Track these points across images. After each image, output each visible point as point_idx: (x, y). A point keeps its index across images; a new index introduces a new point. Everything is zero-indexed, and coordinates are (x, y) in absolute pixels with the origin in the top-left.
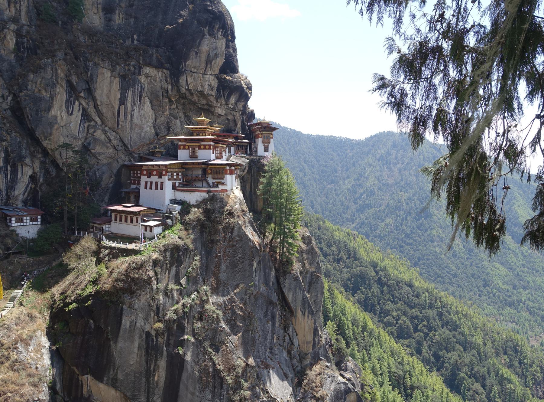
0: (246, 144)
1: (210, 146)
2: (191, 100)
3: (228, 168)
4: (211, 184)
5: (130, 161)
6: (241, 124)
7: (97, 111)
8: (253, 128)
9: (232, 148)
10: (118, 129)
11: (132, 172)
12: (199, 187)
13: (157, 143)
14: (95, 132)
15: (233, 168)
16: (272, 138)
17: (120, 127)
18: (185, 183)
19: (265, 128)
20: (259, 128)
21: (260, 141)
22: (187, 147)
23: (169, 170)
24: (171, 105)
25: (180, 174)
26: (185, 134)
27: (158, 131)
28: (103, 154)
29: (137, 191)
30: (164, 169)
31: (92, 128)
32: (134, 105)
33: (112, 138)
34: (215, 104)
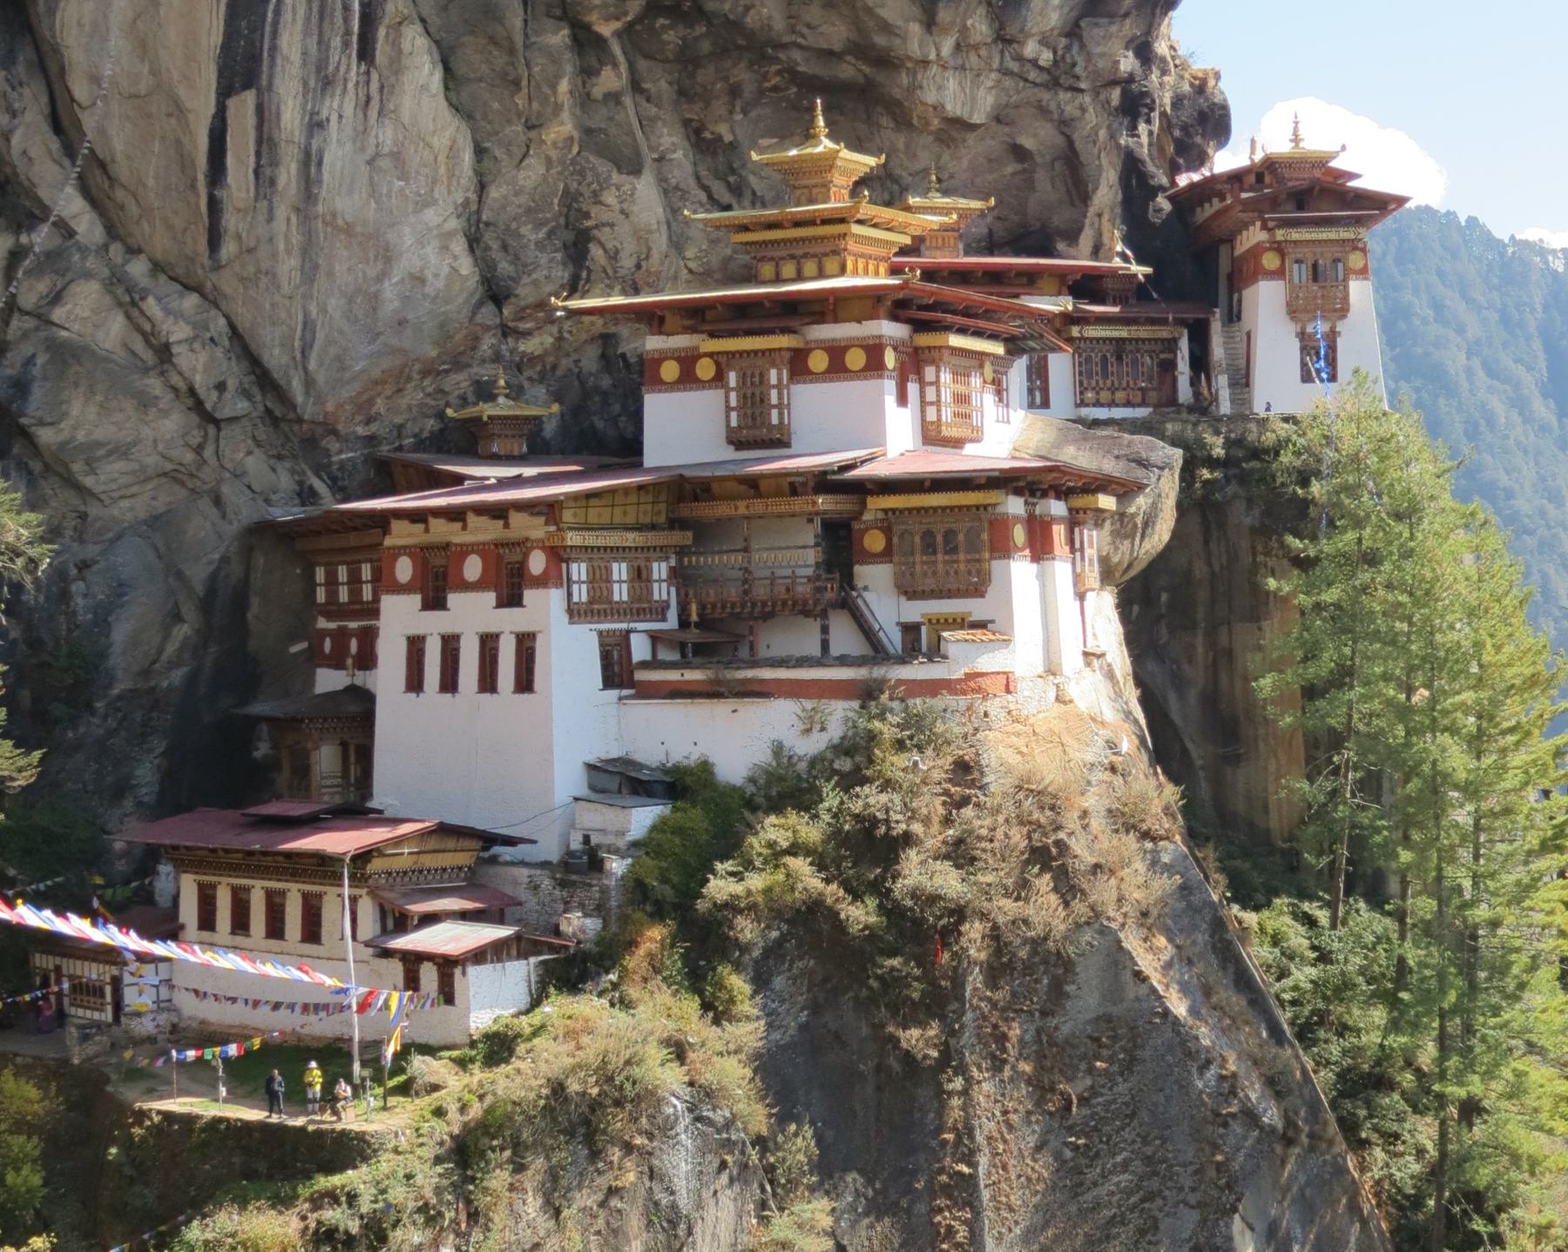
0: (1164, 332)
1: (874, 351)
2: (735, 26)
3: (1015, 506)
4: (893, 639)
5: (306, 495)
7: (70, 151)
8: (1208, 211)
10: (217, 267)
11: (320, 575)
12: (803, 662)
13: (497, 358)
14: (56, 298)
15: (1057, 508)
16: (1363, 272)
17: (228, 249)
18: (693, 636)
19: (1301, 198)
21: (1266, 302)
22: (705, 369)
23: (573, 539)
24: (587, 72)
26: (704, 278)
27: (504, 267)
28: (121, 451)
29: (354, 708)
31: (37, 271)
32: (327, 83)
33: (177, 332)
34: (914, 41)
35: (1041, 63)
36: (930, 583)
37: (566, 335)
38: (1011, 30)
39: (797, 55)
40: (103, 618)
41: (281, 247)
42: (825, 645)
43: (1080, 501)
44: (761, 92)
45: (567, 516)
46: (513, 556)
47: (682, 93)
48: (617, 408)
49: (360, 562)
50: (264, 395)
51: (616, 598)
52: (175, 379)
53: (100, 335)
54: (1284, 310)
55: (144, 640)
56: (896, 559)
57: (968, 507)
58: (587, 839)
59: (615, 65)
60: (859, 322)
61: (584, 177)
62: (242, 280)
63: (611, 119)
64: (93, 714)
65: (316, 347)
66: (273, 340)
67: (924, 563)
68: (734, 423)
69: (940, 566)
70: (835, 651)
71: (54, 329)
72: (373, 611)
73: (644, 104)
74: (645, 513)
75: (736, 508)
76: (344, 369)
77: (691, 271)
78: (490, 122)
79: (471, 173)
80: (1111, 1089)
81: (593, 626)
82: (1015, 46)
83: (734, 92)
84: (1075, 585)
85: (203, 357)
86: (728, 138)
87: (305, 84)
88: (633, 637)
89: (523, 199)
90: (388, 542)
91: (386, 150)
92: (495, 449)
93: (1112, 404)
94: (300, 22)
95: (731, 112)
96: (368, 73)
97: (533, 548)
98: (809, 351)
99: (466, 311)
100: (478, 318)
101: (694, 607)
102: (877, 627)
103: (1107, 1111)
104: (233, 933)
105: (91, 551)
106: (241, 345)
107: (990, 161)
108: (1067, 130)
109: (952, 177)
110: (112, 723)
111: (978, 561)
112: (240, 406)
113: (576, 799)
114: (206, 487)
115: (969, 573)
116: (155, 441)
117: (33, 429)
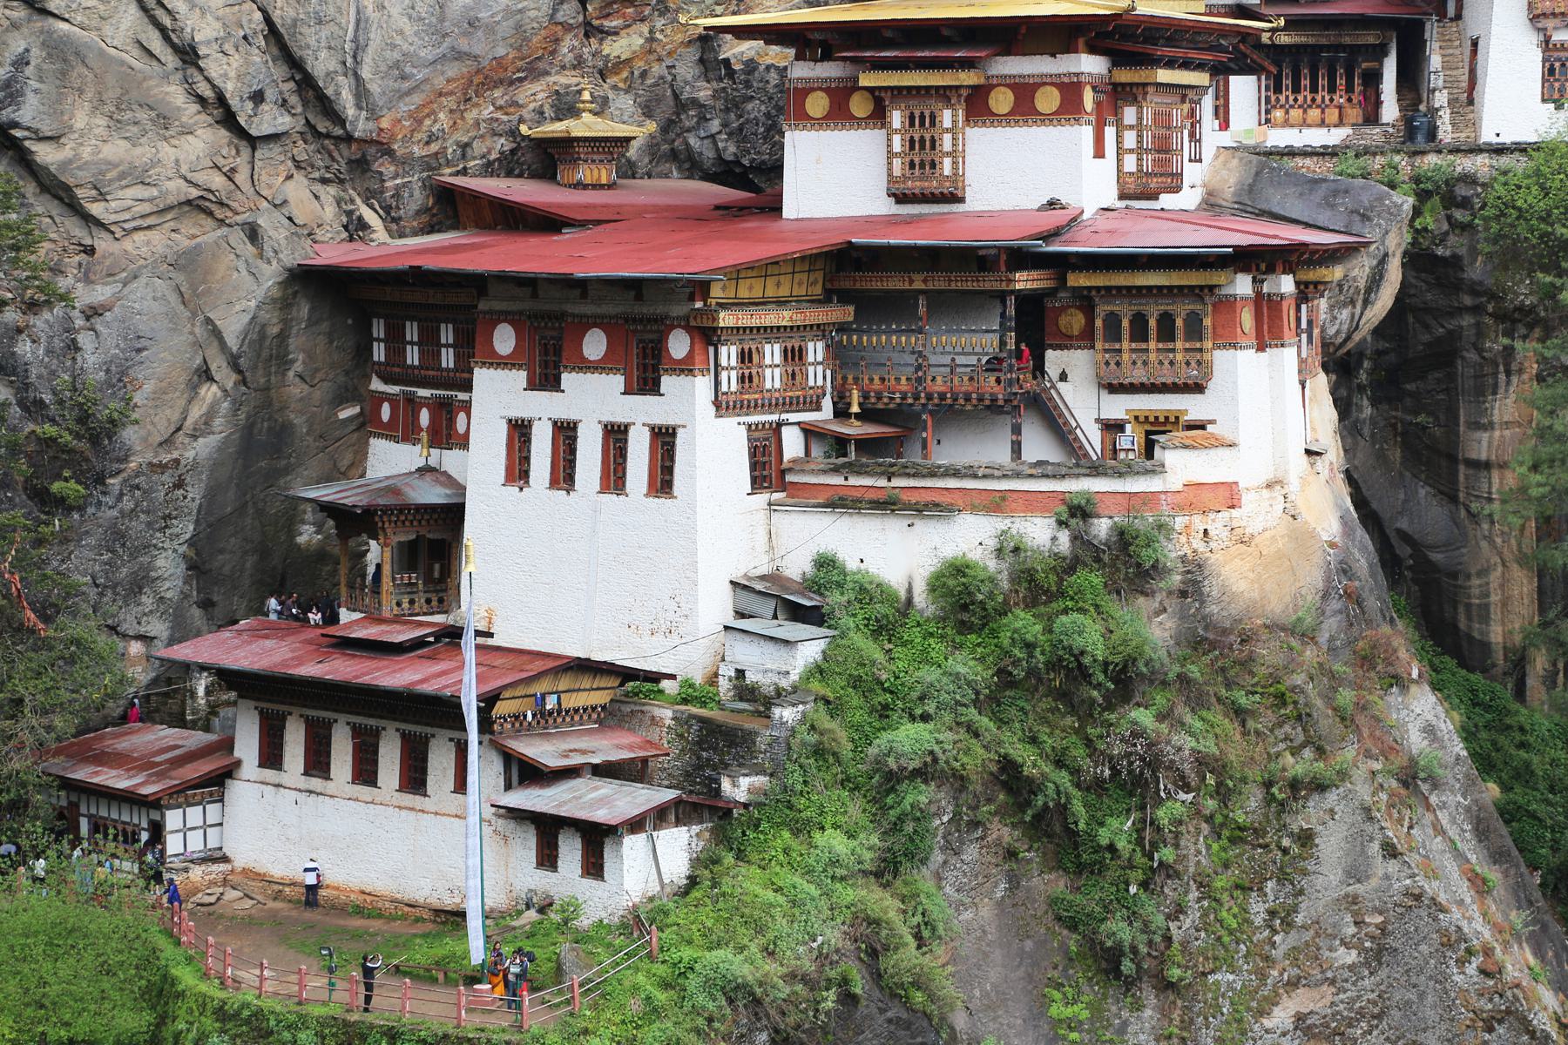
0: (1371, 38)
1: (1070, 90)
3: (1243, 285)
4: (1093, 438)
5: (356, 228)
11: (378, 329)
13: (579, 64)
18: (854, 429)
22: (859, 106)
23: (726, 319)
30: (678, 310)
36: (1139, 375)
37: (658, 36)
40: (119, 377)
43: (1311, 275)
45: (716, 292)
48: (715, 125)
49: (439, 321)
50: (305, 104)
51: (768, 385)
52: (205, 90)
53: (108, 30)
56: (1099, 345)
57: (1191, 288)
58: (740, 673)
60: (1053, 55)
64: (104, 493)
65: (370, 50)
67: (1133, 351)
68: (897, 172)
69: (1153, 356)
71: (51, 20)
72: (467, 386)
74: (800, 284)
75: (911, 282)
76: (404, 78)
80: (1354, 984)
84: (1300, 372)
85: (236, 60)
88: (784, 429)
90: (483, 305)
92: (579, 176)
93: (1304, 124)
97: (673, 327)
98: (993, 87)
101: (855, 396)
103: (1350, 1010)
104: (306, 773)
105: (101, 293)
110: (127, 503)
111: (1201, 350)
112: (280, 120)
113: (726, 628)
114: (239, 219)
115: (1188, 364)
116: (177, 161)
117: (27, 143)
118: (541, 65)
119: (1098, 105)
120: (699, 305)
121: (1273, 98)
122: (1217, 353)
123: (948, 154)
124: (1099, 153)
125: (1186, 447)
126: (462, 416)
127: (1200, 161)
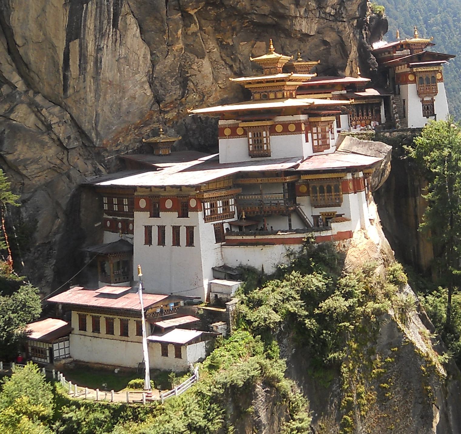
1: (298, 125)
3: (349, 176)
4: (311, 221)
6: (359, 50)
9: (344, 118)
11: (105, 200)
13: (158, 121)
18: (244, 223)
20: (407, 61)
22: (240, 132)
23: (206, 195)
25: (232, 201)
27: (161, 91)
29: (126, 249)
30: (193, 193)
32: (103, 35)
33: (54, 120)
34: (293, 10)
35: (332, 14)
36: (322, 203)
37: (180, 112)
38: (323, 5)
39: (254, 17)
41: (88, 90)
42: (290, 225)
44: (241, 28)
46: (185, 200)
47: (215, 30)
48: (197, 136)
51: (219, 213)
54: (418, 96)
55: (49, 225)
56: (311, 195)
58: (216, 296)
59: (195, 24)
60: (293, 116)
61: (186, 60)
62: (75, 101)
63: (194, 41)
66: (85, 121)
67: (321, 196)
69: (326, 197)
70: (293, 228)
72: (133, 216)
73: (204, 34)
75: (258, 181)
76: (109, 129)
77: (220, 88)
78: (156, 45)
79: (150, 62)
81: (212, 223)
82: (324, 9)
83: (234, 29)
86: (231, 44)
87: (95, 36)
88: (224, 224)
89: (167, 69)
91: (123, 56)
92: (161, 153)
94: (93, 16)
95: (232, 36)
96: (116, 31)
99: (149, 107)
100: (153, 109)
102: (305, 217)
106: (76, 124)
107: (316, 46)
108: (339, 34)
109: (304, 52)
112: (75, 144)
115: (336, 199)
118: (148, 122)
119: (306, 128)
120: (198, 192)
121: (352, 119)
122: (344, 196)
123: (265, 144)
124: (307, 141)
125: (337, 222)
126: (131, 225)
127: (334, 139)
